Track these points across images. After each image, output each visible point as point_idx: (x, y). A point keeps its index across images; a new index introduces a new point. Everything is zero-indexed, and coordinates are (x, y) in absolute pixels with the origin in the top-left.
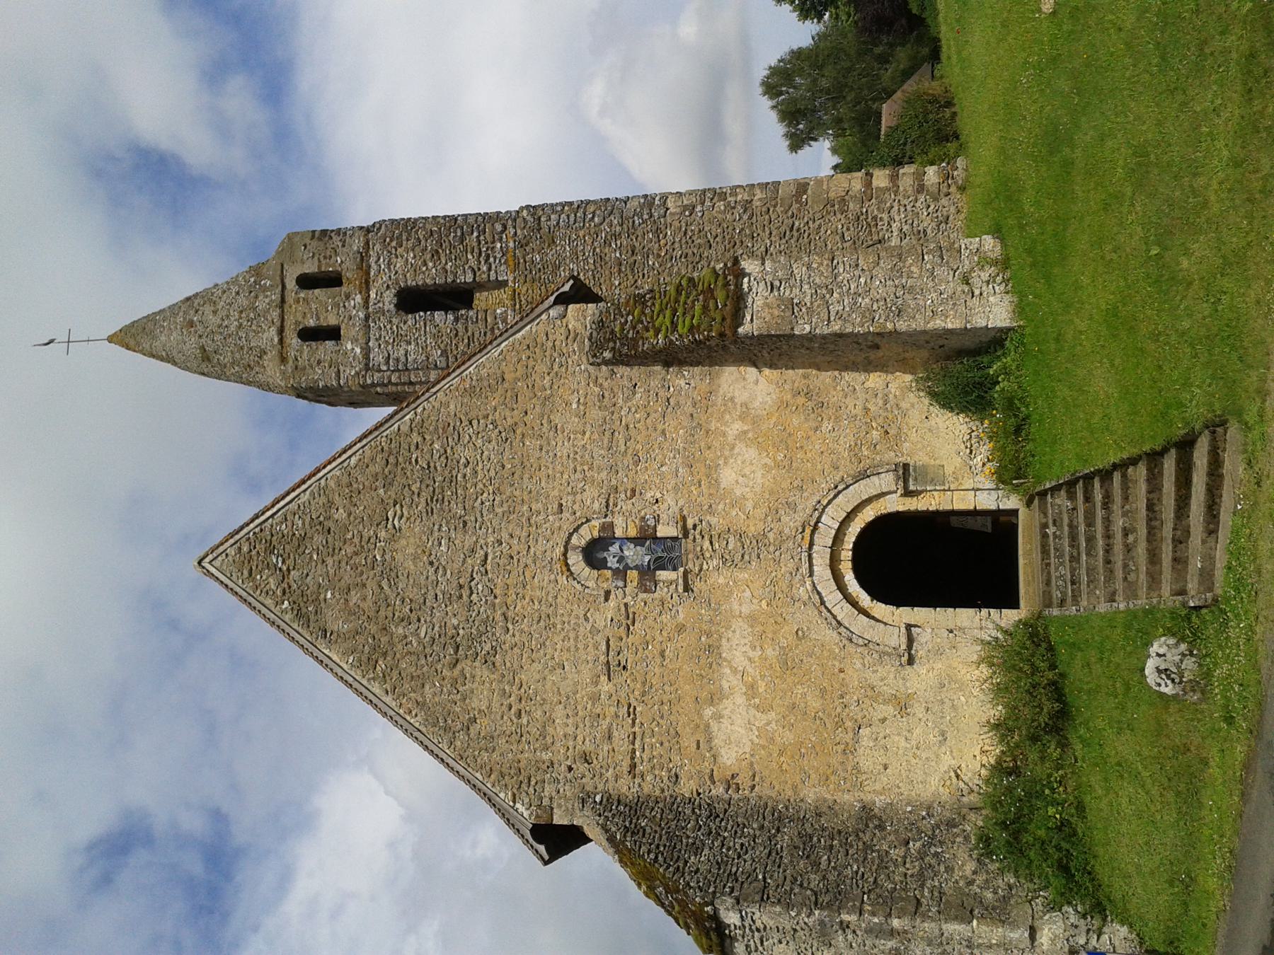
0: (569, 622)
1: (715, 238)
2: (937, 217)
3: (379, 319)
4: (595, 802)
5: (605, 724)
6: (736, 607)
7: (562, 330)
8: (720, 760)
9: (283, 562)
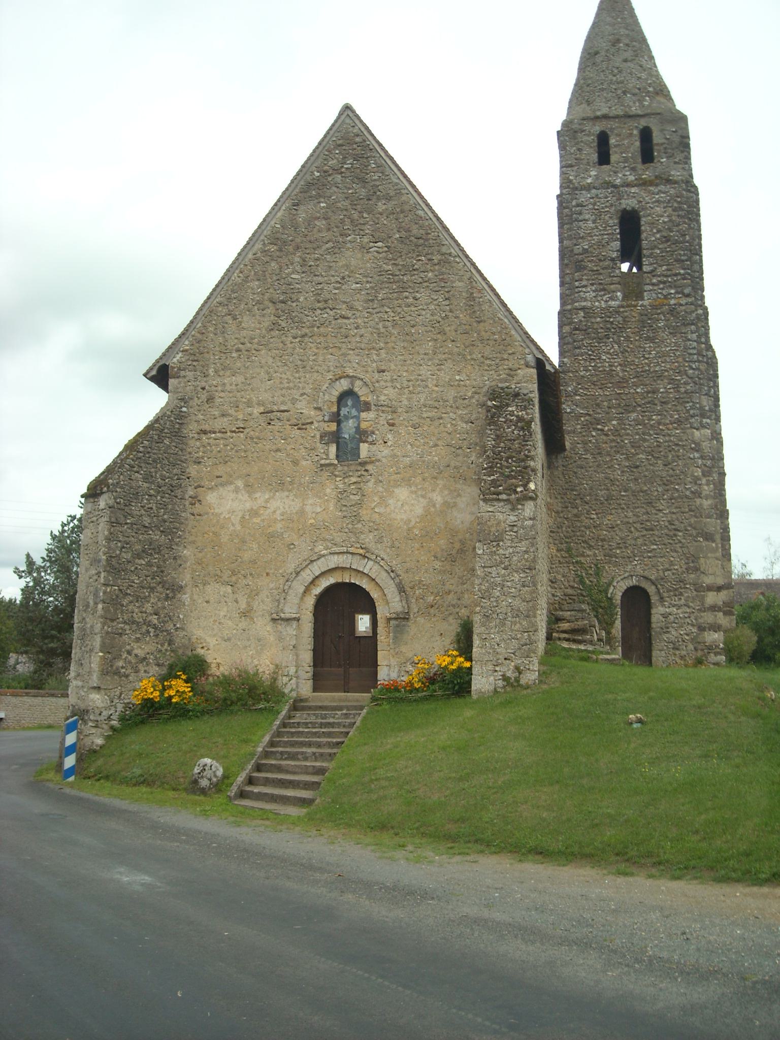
0: (300, 382)
1: (672, 469)
2: (678, 641)
3: (613, 196)
4: (181, 408)
5: (232, 412)
6: (310, 501)
7: (517, 366)
8: (210, 492)
9: (347, 168)
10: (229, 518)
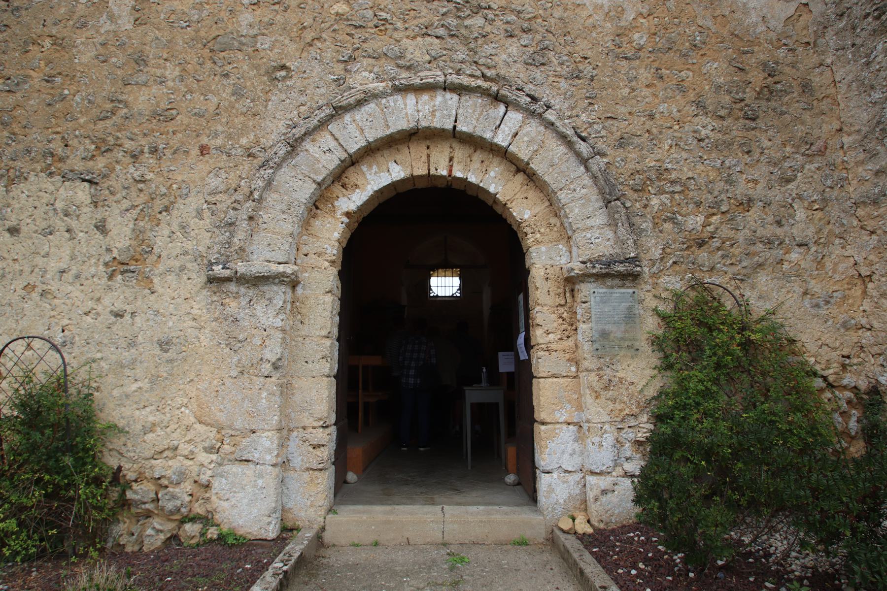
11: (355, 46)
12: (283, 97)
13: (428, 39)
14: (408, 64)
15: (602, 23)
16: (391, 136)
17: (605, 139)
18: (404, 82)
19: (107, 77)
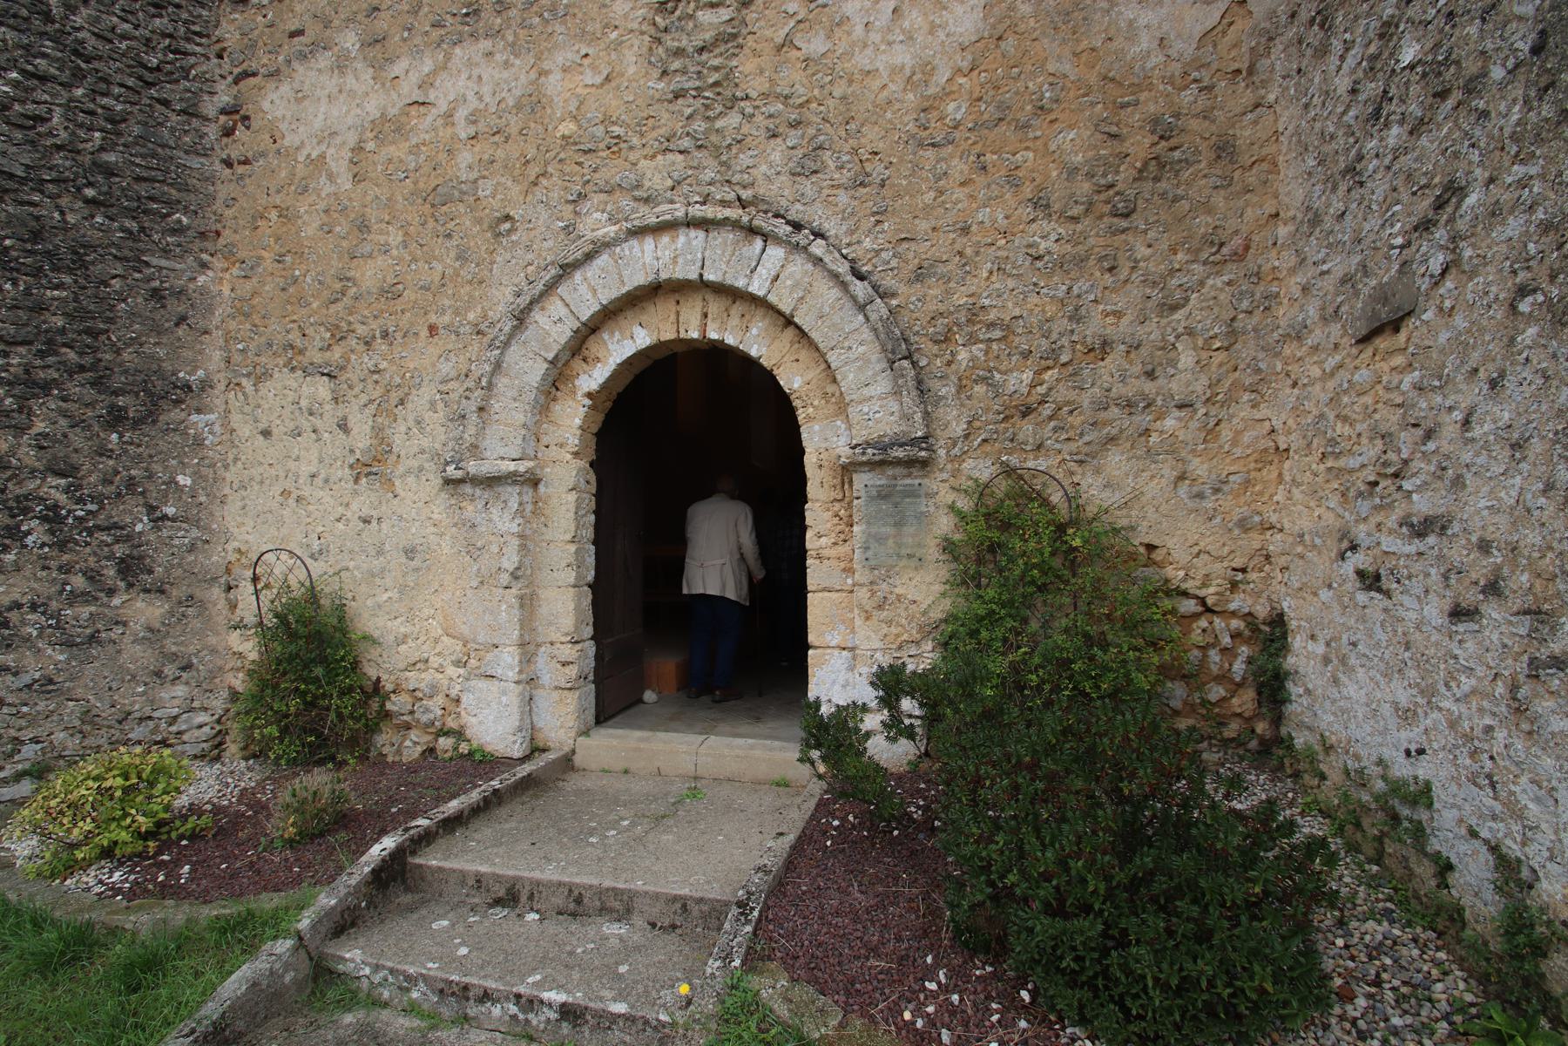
8: (271, 85)
10: (322, 156)
11: (585, 178)
12: (508, 256)
13: (670, 156)
14: (645, 195)
15: (900, 96)
16: (629, 293)
17: (896, 272)
18: (636, 223)
19: (333, 252)
